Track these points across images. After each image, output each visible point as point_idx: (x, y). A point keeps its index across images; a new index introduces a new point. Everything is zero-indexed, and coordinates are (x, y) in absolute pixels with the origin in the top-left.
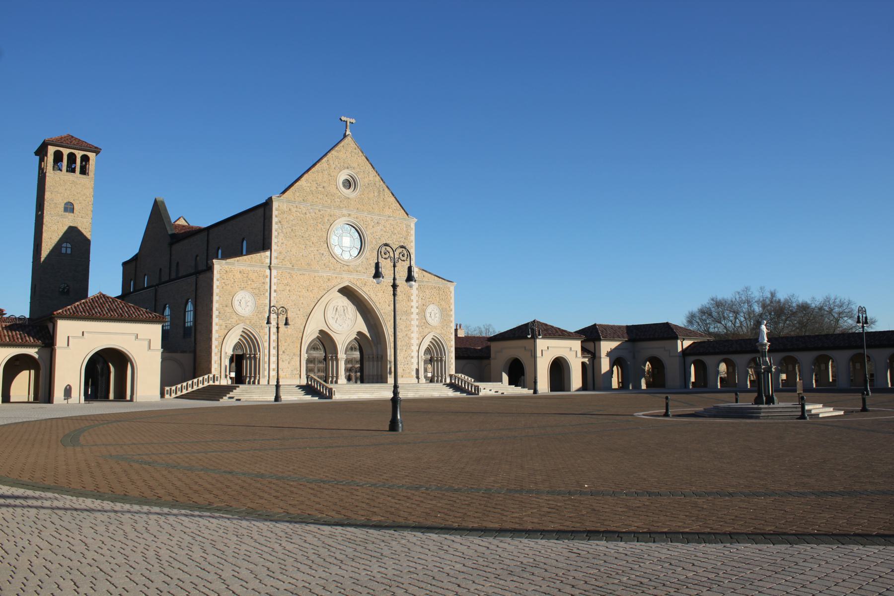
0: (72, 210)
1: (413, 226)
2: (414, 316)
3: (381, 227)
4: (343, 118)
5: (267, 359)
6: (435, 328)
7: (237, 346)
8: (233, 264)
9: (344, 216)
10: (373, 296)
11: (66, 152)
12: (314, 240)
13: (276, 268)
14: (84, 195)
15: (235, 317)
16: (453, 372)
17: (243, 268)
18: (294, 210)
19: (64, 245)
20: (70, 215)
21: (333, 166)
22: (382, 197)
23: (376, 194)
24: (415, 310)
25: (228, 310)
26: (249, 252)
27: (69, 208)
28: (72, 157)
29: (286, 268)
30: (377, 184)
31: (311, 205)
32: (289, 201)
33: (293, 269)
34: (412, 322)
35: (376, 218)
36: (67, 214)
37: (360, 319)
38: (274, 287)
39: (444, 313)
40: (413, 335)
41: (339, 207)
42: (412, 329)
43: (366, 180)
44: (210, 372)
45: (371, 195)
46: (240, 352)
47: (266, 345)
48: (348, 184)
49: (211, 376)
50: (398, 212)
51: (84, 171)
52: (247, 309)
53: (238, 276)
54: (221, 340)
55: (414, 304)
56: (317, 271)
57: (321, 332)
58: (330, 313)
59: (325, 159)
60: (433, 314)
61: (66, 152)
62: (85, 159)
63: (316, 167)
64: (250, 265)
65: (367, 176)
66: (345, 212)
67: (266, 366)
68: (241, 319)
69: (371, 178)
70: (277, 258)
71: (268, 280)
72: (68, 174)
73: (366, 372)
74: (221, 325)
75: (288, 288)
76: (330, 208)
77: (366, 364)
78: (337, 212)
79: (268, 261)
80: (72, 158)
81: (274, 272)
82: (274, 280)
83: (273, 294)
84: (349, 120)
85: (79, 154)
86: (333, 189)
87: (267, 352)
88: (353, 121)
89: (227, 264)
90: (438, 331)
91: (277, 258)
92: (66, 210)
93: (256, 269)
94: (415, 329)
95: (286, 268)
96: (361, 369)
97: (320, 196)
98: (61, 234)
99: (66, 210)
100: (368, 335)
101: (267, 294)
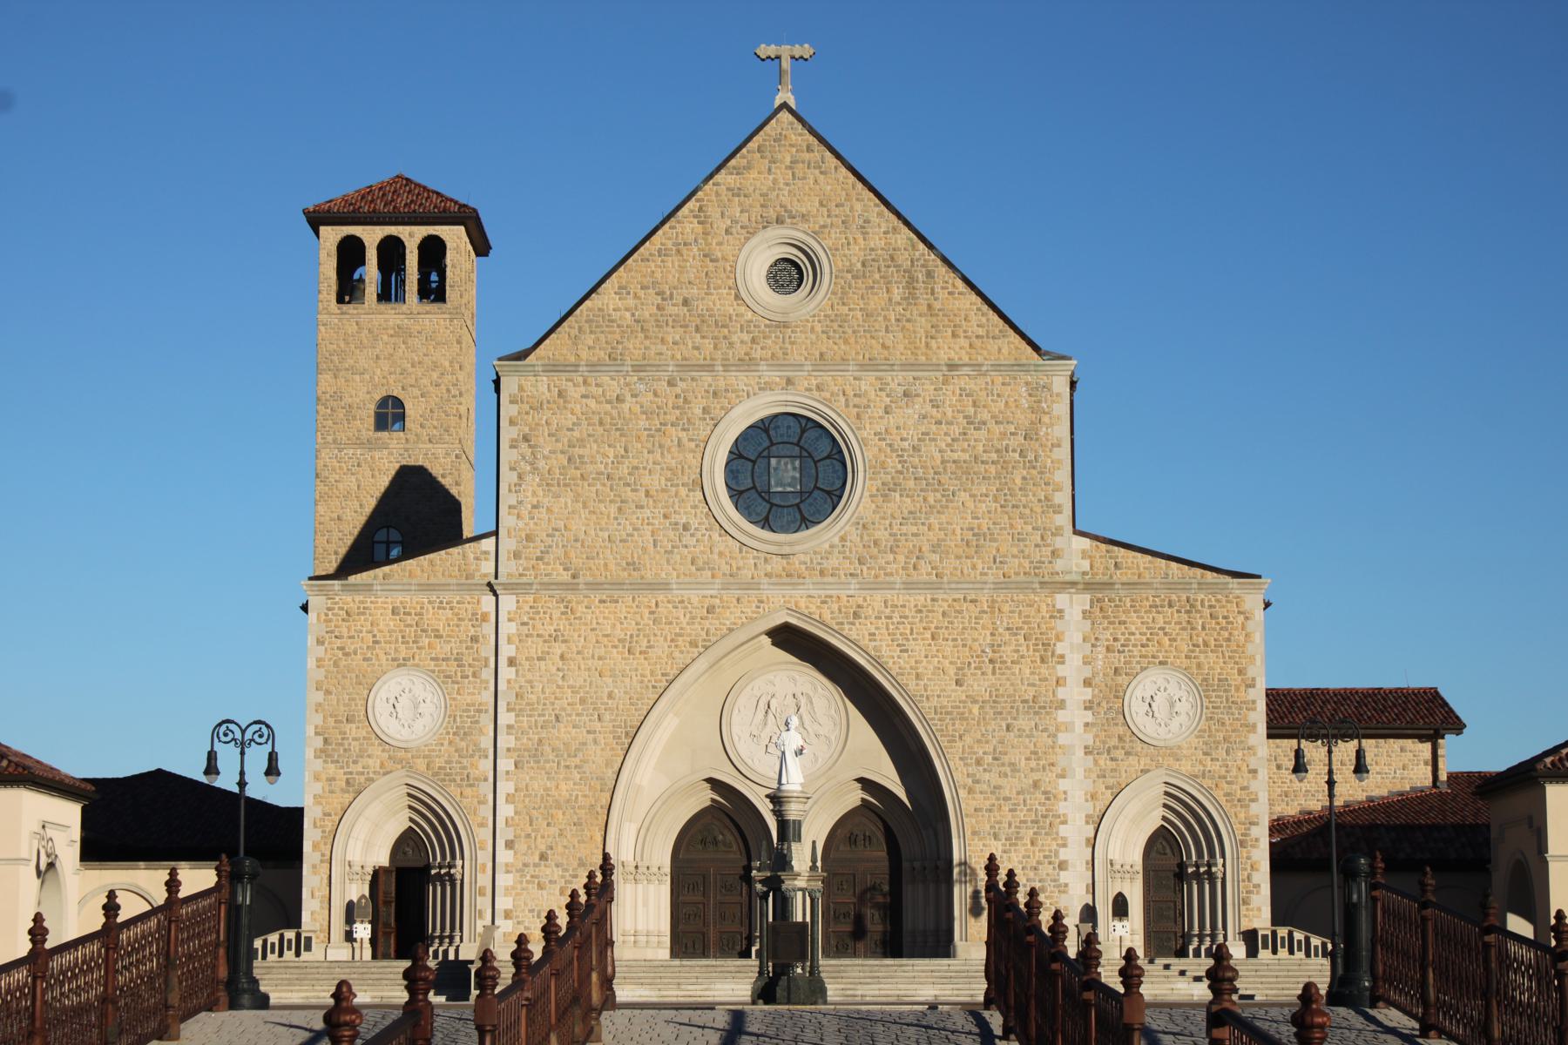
0: (401, 417)
1: (1061, 385)
2: (1074, 718)
3: (918, 406)
4: (765, 50)
5: (484, 880)
6: (1174, 753)
7: (407, 841)
8: (368, 588)
9: (766, 387)
10: (888, 652)
11: (371, 236)
12: (655, 482)
13: (511, 587)
14: (435, 366)
15: (376, 750)
16: (1261, 918)
17: (399, 598)
18: (574, 392)
19: (381, 535)
20: (393, 438)
21: (722, 225)
22: (923, 299)
23: (897, 293)
24: (1074, 694)
25: (351, 730)
26: (408, 554)
27: (390, 414)
28: (391, 252)
29: (546, 586)
30: (903, 259)
31: (637, 368)
32: (553, 368)
33: (571, 587)
34: (1062, 738)
35: (897, 381)
36: (385, 434)
37: (865, 736)
38: (506, 651)
39: (1213, 693)
40: (1063, 784)
41: (747, 363)
42: (1062, 762)
43: (856, 253)
44: (294, 921)
45: (877, 301)
46: (412, 860)
47: (485, 834)
48: (790, 274)
49: (290, 934)
50: (993, 346)
51: (433, 292)
52: (419, 726)
53: (387, 622)
54: (329, 826)
55: (1072, 668)
56: (665, 586)
57: (714, 783)
58: (741, 724)
59: (691, 204)
60: (1164, 705)
61: (371, 236)
62: (433, 252)
63: (656, 238)
64: (426, 587)
65: (853, 231)
66: (774, 376)
67: (484, 903)
68: (398, 756)
69: (877, 241)
70: (517, 555)
71: (489, 629)
72: (383, 306)
73: (908, 923)
74: (331, 780)
75: (558, 649)
76: (709, 368)
77: (908, 891)
78: (740, 380)
79: (488, 567)
80: (391, 252)
81: (508, 602)
82: (507, 628)
83: (506, 673)
84: (785, 51)
85: (412, 236)
86: (722, 303)
87: (484, 857)
88: (806, 50)
89: (345, 589)
90: (1186, 767)
91: (517, 555)
92: (382, 423)
93: (446, 597)
94: (1079, 763)
95: (546, 586)
96: (894, 911)
97: (673, 335)
98: (370, 504)
99: (382, 423)
100: (901, 793)
101: (488, 674)
